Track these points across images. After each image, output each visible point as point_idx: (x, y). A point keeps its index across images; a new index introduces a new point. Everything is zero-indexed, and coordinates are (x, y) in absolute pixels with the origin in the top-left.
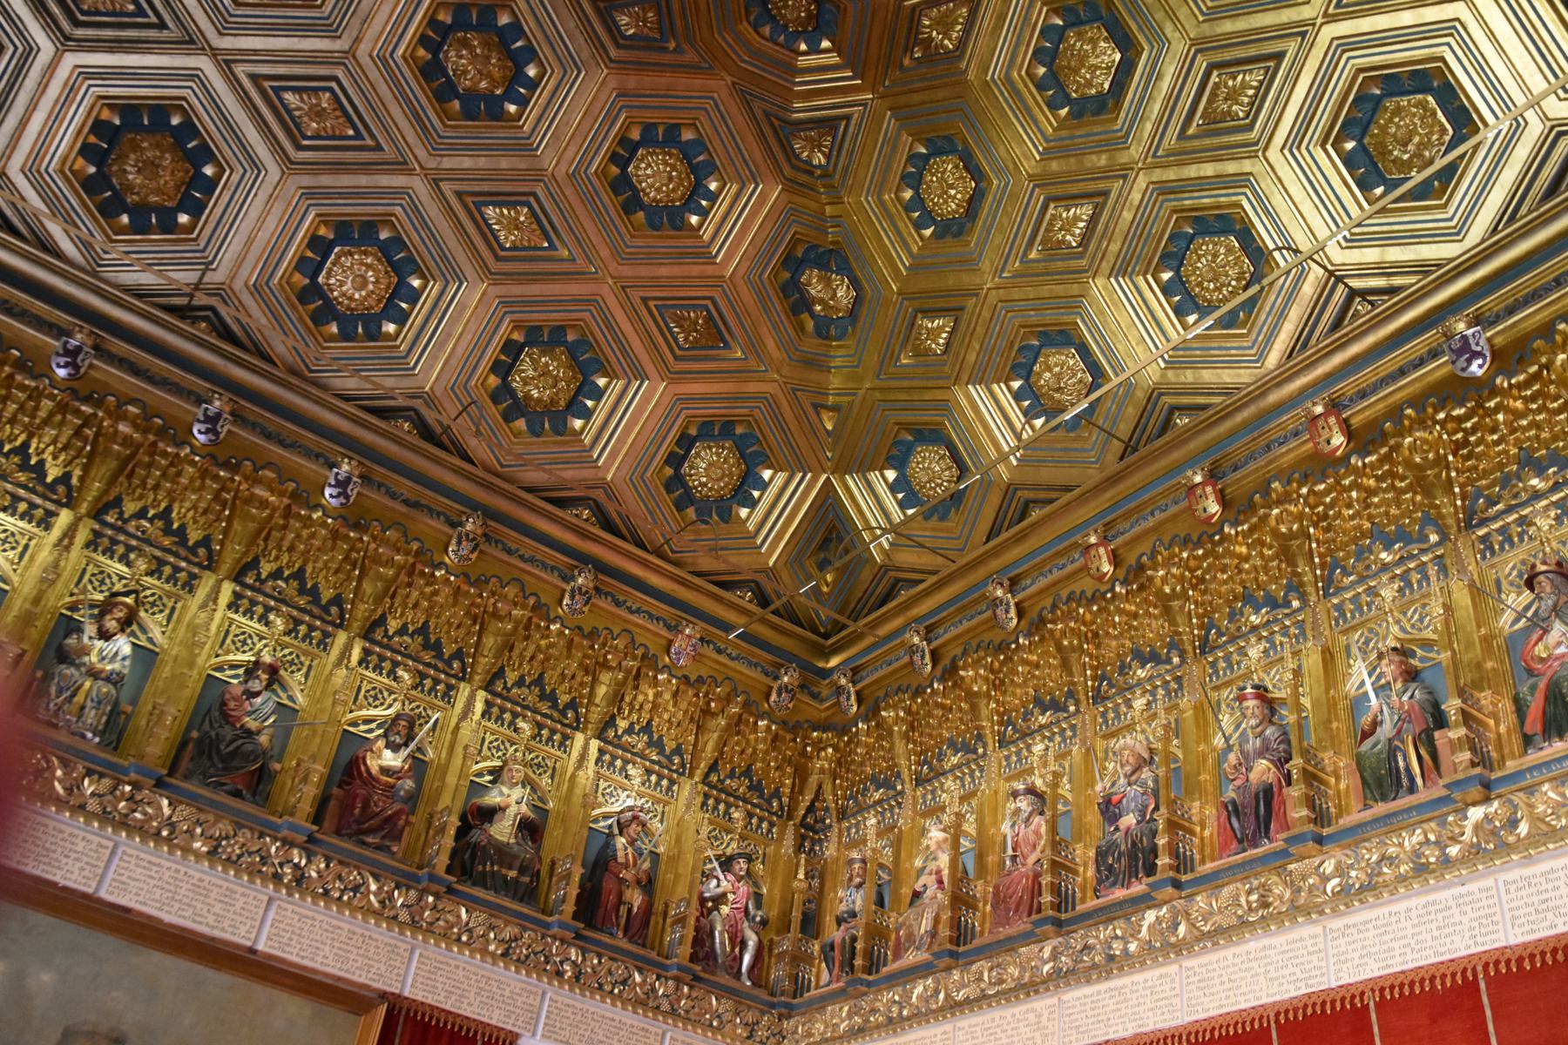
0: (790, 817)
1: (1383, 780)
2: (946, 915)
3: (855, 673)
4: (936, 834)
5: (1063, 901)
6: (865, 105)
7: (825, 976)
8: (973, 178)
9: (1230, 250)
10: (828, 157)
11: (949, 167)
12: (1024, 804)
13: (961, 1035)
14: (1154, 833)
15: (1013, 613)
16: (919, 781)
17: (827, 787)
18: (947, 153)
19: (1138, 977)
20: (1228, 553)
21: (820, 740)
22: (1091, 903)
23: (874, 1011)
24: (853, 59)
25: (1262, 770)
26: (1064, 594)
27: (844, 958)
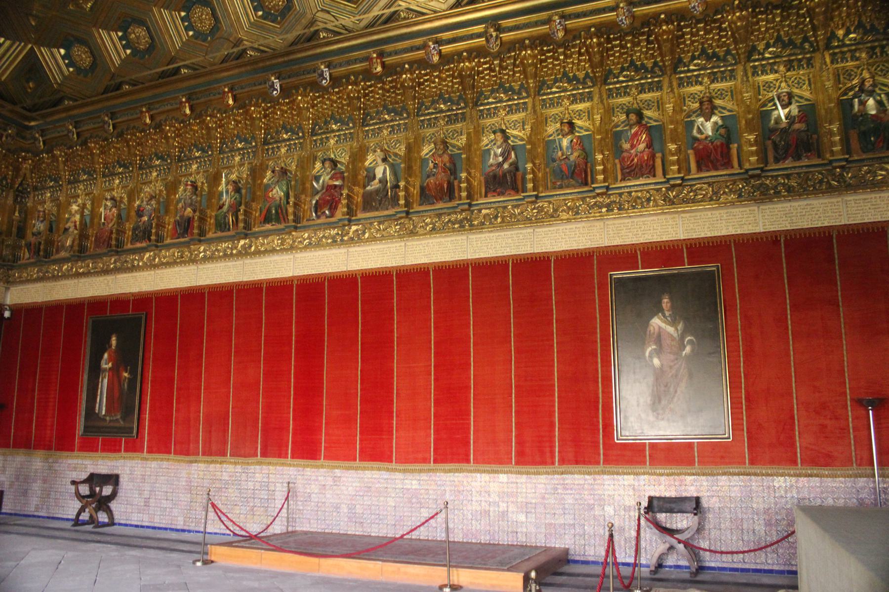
0: (11, 188)
1: (222, 225)
2: (76, 242)
3: (43, 132)
4: (75, 207)
5: (120, 243)
7: (27, 255)
9: (207, 14)
12: (109, 204)
13: (80, 285)
14: (152, 228)
15: (111, 127)
16: (70, 182)
17: (28, 175)
19: (142, 273)
20: (191, 130)
21: (25, 156)
22: (129, 246)
23: (47, 272)
26: (132, 125)
27: (35, 250)
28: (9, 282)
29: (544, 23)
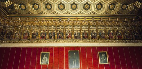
25: (44, 35)
28: (2, 43)
29: (100, 18)
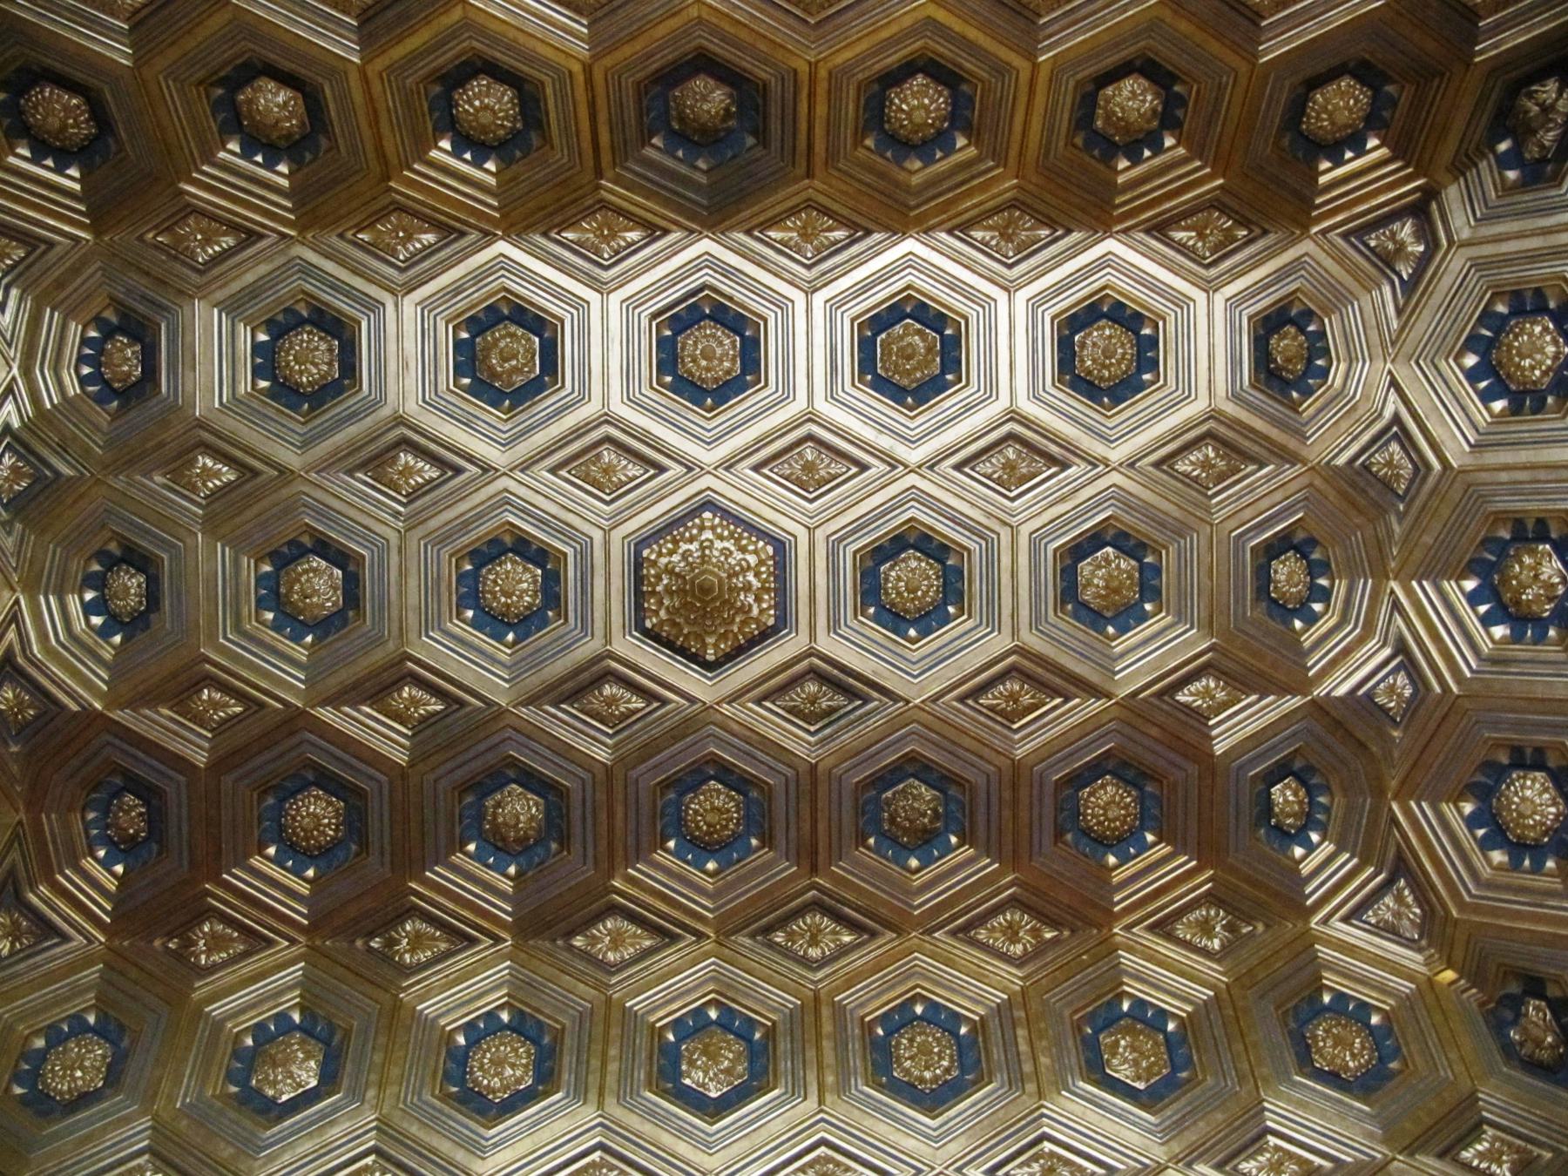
6: (90, 942)
8: (105, 1079)
10: (12, 953)
11: (99, 1052)
18: (107, 1040)
24: (122, 899)
